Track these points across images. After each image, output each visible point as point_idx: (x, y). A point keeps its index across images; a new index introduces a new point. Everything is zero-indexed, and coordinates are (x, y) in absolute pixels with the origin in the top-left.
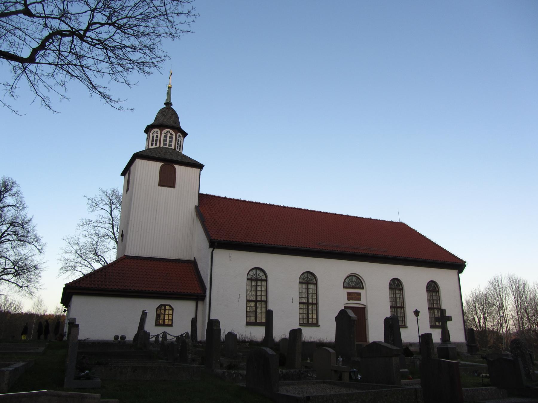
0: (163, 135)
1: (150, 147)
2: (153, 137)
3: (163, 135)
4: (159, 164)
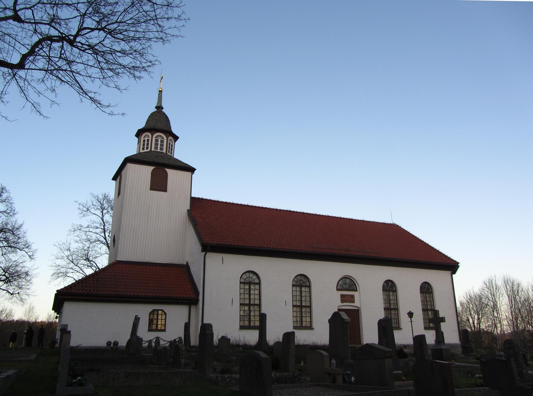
0: (154, 139)
1: (141, 151)
2: (144, 141)
3: (154, 139)
4: (151, 168)
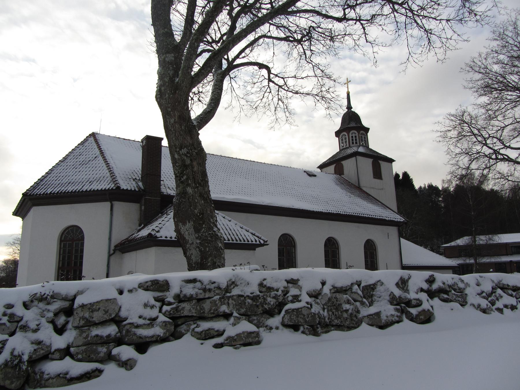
2: (352, 137)
